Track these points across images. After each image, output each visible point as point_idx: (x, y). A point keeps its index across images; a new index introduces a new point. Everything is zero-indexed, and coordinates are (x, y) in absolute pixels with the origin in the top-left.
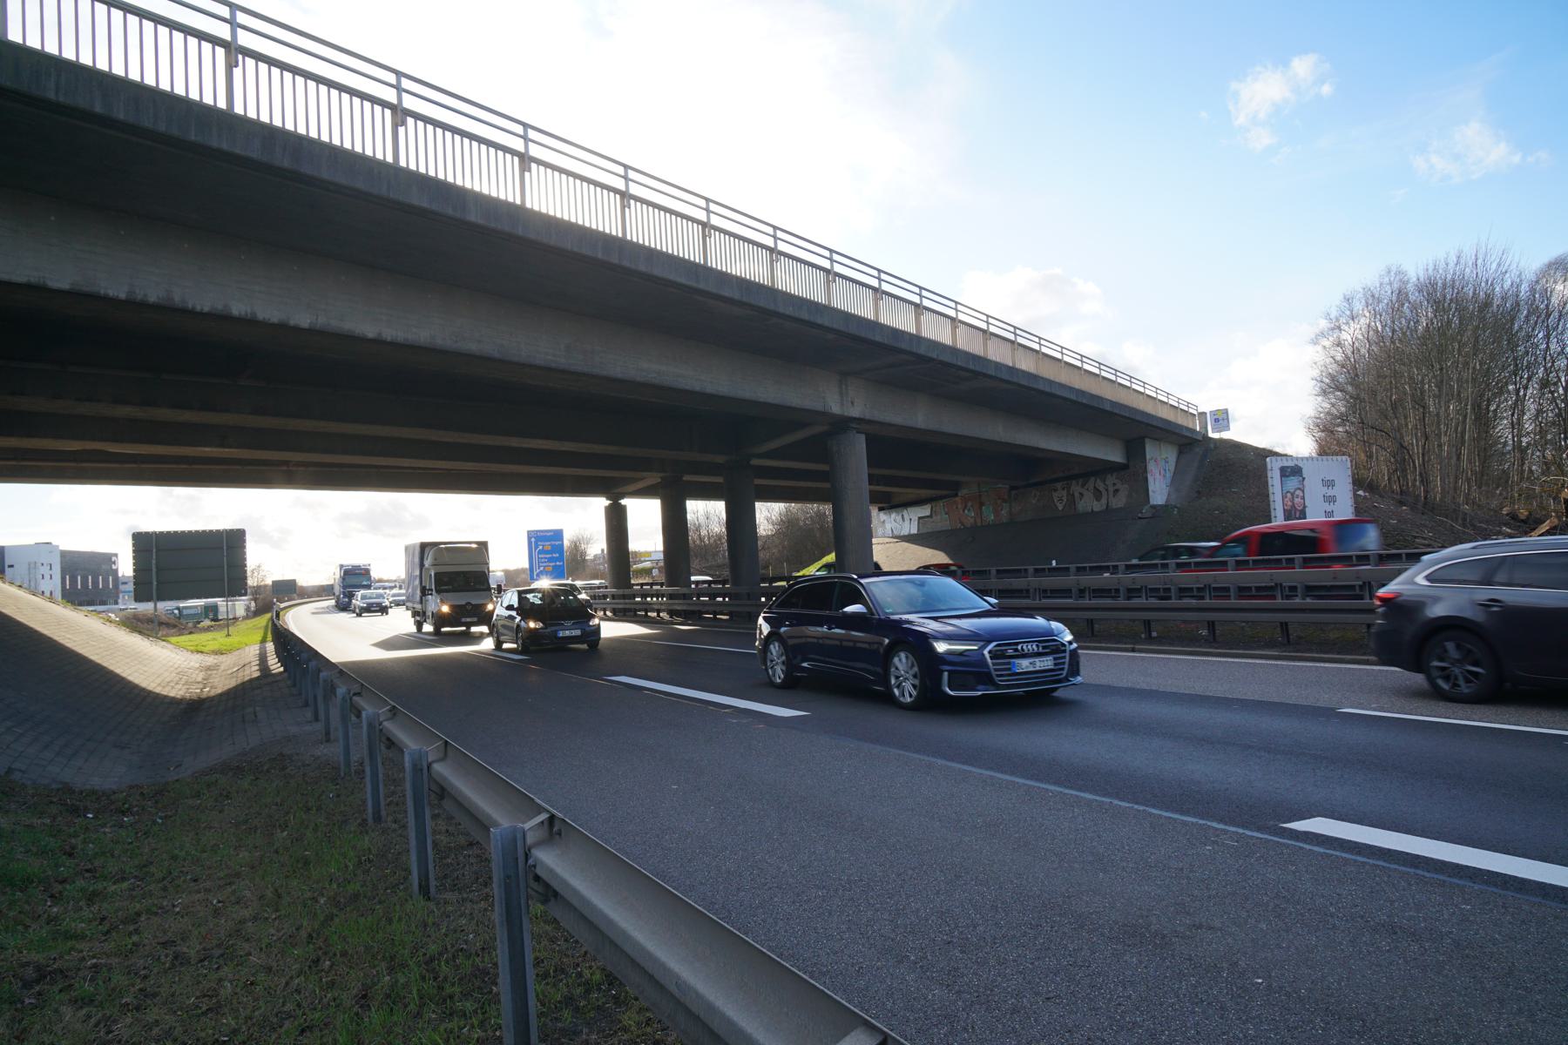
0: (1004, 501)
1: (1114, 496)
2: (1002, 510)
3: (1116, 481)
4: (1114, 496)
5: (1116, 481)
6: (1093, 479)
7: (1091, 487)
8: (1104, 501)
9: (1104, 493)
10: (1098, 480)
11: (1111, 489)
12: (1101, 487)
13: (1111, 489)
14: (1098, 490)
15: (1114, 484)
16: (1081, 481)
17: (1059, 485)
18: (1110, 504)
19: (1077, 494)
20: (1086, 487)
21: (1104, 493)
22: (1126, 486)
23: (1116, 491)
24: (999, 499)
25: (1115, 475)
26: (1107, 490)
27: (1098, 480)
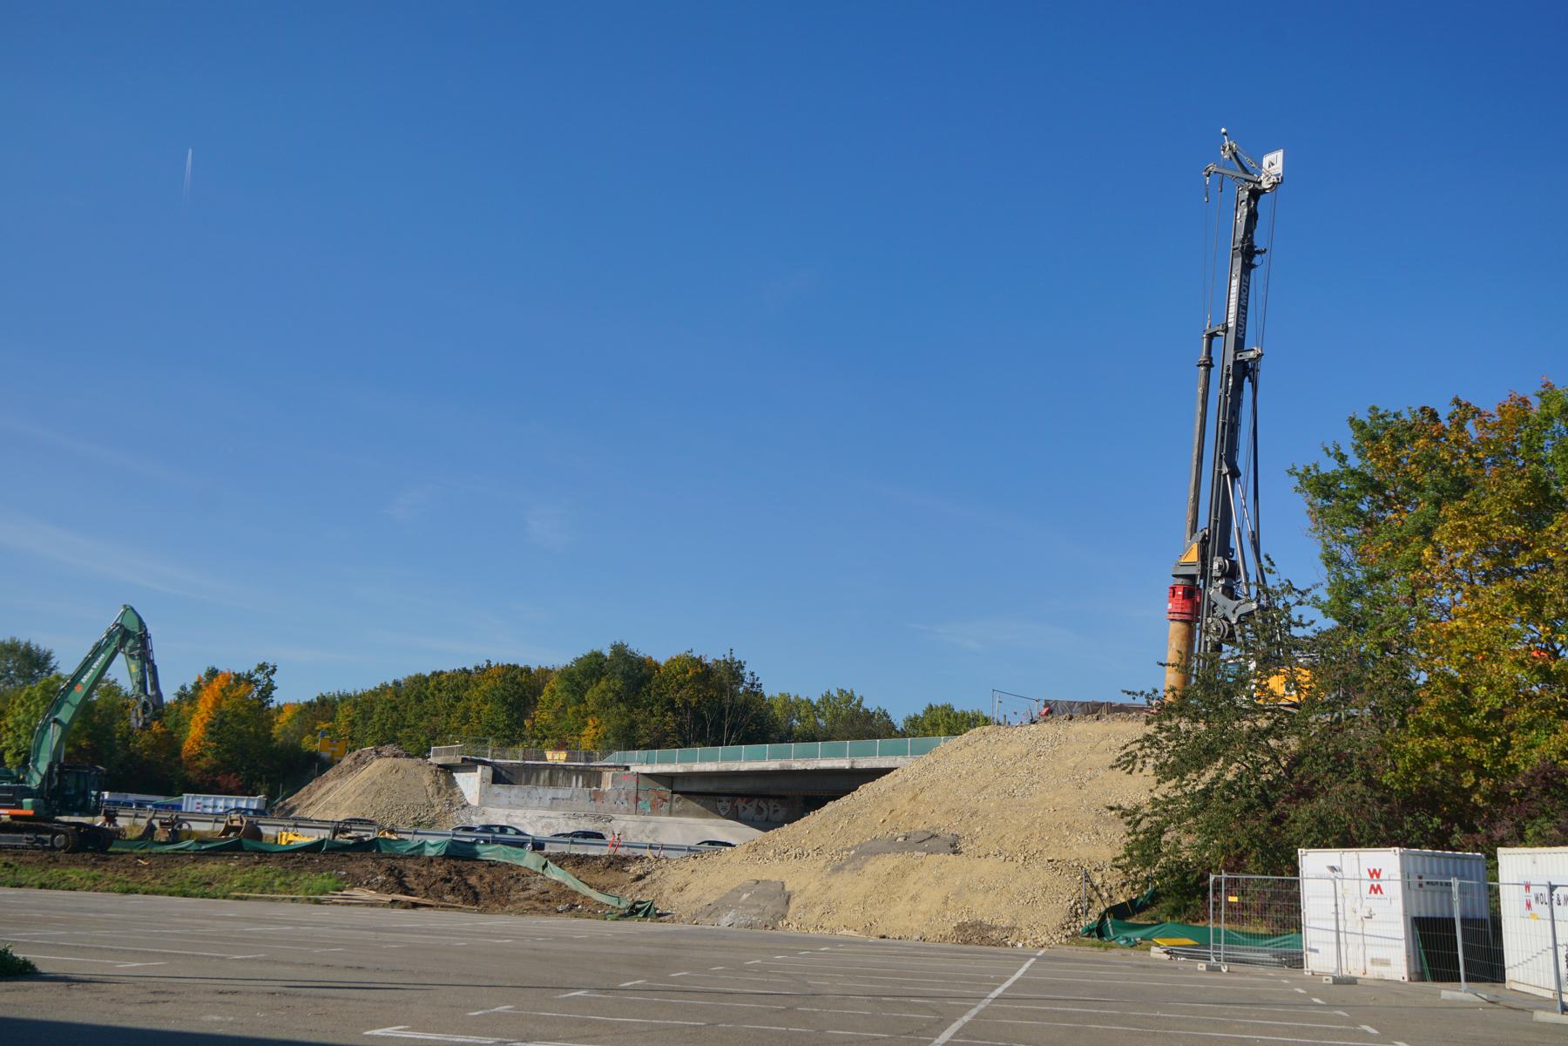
0: (665, 800)
6: (757, 800)
10: (761, 802)
12: (763, 805)
13: (772, 810)
15: (775, 806)
16: (745, 799)
17: (724, 799)
19: (740, 808)
23: (776, 811)
26: (768, 809)
27: (761, 802)
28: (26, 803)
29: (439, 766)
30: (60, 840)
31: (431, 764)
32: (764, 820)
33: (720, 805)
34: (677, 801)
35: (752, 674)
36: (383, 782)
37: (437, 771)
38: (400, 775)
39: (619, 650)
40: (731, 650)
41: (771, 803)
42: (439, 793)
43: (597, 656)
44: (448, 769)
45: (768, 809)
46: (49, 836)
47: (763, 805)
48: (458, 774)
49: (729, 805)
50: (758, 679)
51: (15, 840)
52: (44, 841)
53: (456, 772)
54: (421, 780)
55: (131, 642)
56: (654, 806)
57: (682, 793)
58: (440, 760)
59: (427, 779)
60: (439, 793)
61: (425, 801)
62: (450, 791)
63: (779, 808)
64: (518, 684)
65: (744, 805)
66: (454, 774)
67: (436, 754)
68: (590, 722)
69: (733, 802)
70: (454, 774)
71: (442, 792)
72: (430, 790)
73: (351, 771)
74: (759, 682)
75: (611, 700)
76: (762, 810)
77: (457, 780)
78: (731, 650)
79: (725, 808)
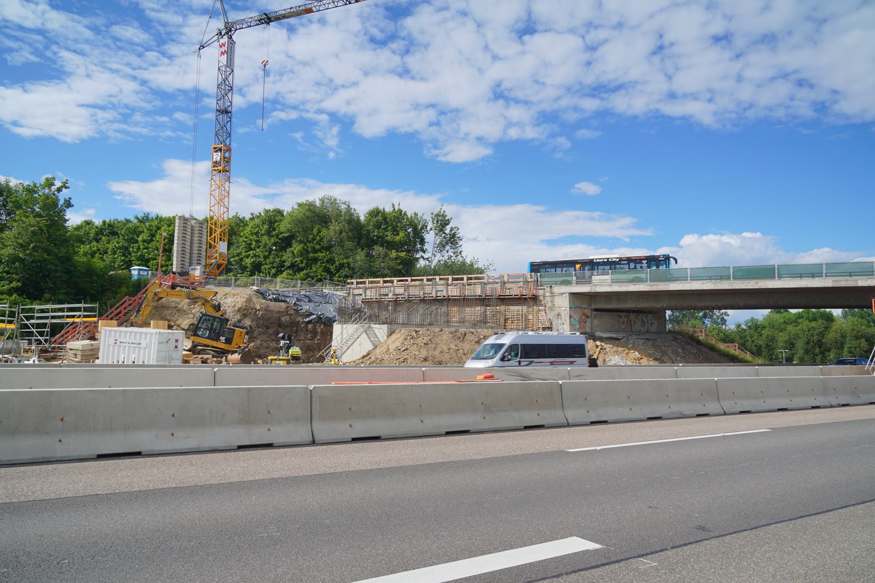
0: (587, 317)
1: (651, 326)
2: (585, 323)
3: (653, 318)
4: (651, 326)
6: (641, 315)
7: (640, 320)
8: (646, 328)
10: (644, 317)
11: (650, 322)
12: (645, 320)
13: (650, 322)
14: (643, 321)
15: (651, 320)
17: (623, 314)
19: (632, 321)
20: (638, 318)
21: (646, 323)
22: (656, 322)
23: (652, 323)
24: (584, 315)
25: (652, 315)
26: (648, 322)
27: (644, 317)
32: (646, 331)
33: (621, 320)
34: (595, 318)
41: (650, 317)
45: (648, 322)
49: (626, 319)
56: (581, 322)
57: (596, 310)
63: (653, 321)
65: (635, 320)
69: (628, 317)
76: (645, 323)
79: (623, 323)
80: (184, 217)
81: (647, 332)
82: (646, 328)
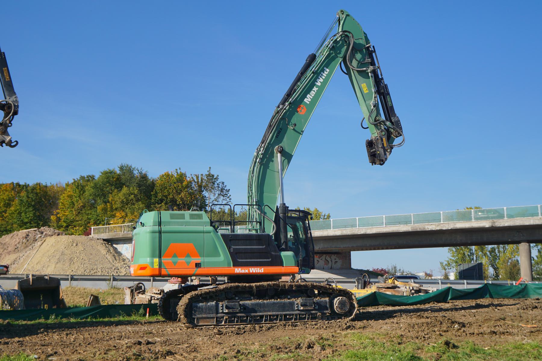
3: (336, 258)
5: (336, 258)
6: (324, 255)
7: (324, 259)
9: (330, 262)
11: (334, 261)
12: (329, 259)
13: (334, 261)
14: (327, 260)
15: (335, 259)
16: (318, 255)
18: (333, 267)
20: (321, 258)
21: (330, 262)
22: (341, 260)
23: (336, 262)
25: (336, 255)
26: (331, 261)
28: (286, 256)
29: (104, 240)
30: (342, 304)
31: (98, 239)
35: (223, 183)
36: (70, 253)
37: (105, 244)
38: (80, 248)
39: (127, 170)
40: (210, 168)
41: (333, 257)
42: (116, 259)
43: (111, 172)
44: (110, 242)
45: (331, 261)
46: (327, 299)
47: (329, 259)
48: (119, 245)
50: (226, 186)
51: (283, 307)
52: (321, 307)
53: (117, 244)
54: (98, 251)
55: (359, 56)
58: (106, 236)
59: (102, 249)
60: (116, 259)
61: (109, 266)
62: (121, 258)
64: (37, 193)
66: (114, 245)
67: (98, 231)
68: (118, 214)
70: (114, 245)
71: (117, 258)
72: (109, 257)
73: (27, 247)
74: (227, 188)
75: (132, 200)
77: (119, 250)
78: (210, 168)
80: (19, 183)
81: (331, 268)
82: (330, 265)
